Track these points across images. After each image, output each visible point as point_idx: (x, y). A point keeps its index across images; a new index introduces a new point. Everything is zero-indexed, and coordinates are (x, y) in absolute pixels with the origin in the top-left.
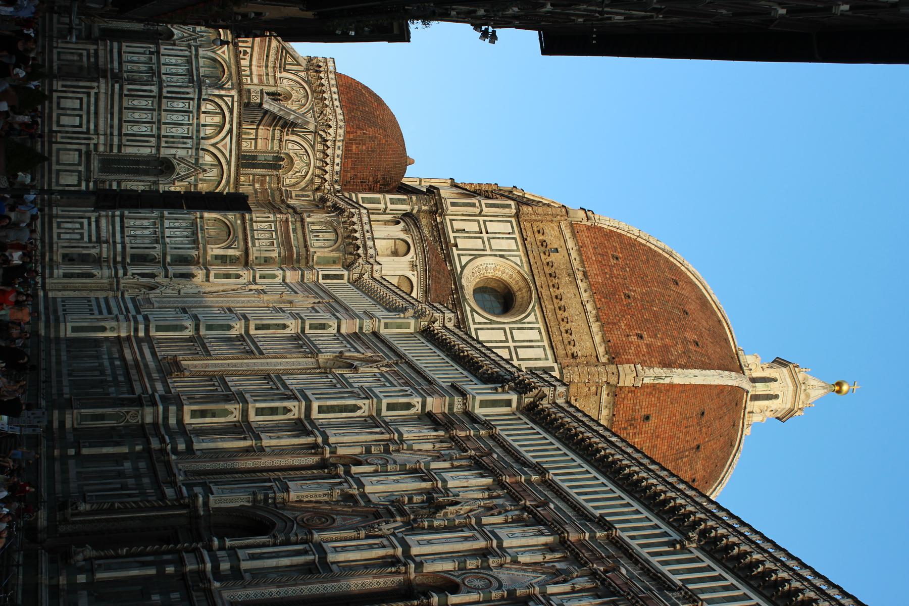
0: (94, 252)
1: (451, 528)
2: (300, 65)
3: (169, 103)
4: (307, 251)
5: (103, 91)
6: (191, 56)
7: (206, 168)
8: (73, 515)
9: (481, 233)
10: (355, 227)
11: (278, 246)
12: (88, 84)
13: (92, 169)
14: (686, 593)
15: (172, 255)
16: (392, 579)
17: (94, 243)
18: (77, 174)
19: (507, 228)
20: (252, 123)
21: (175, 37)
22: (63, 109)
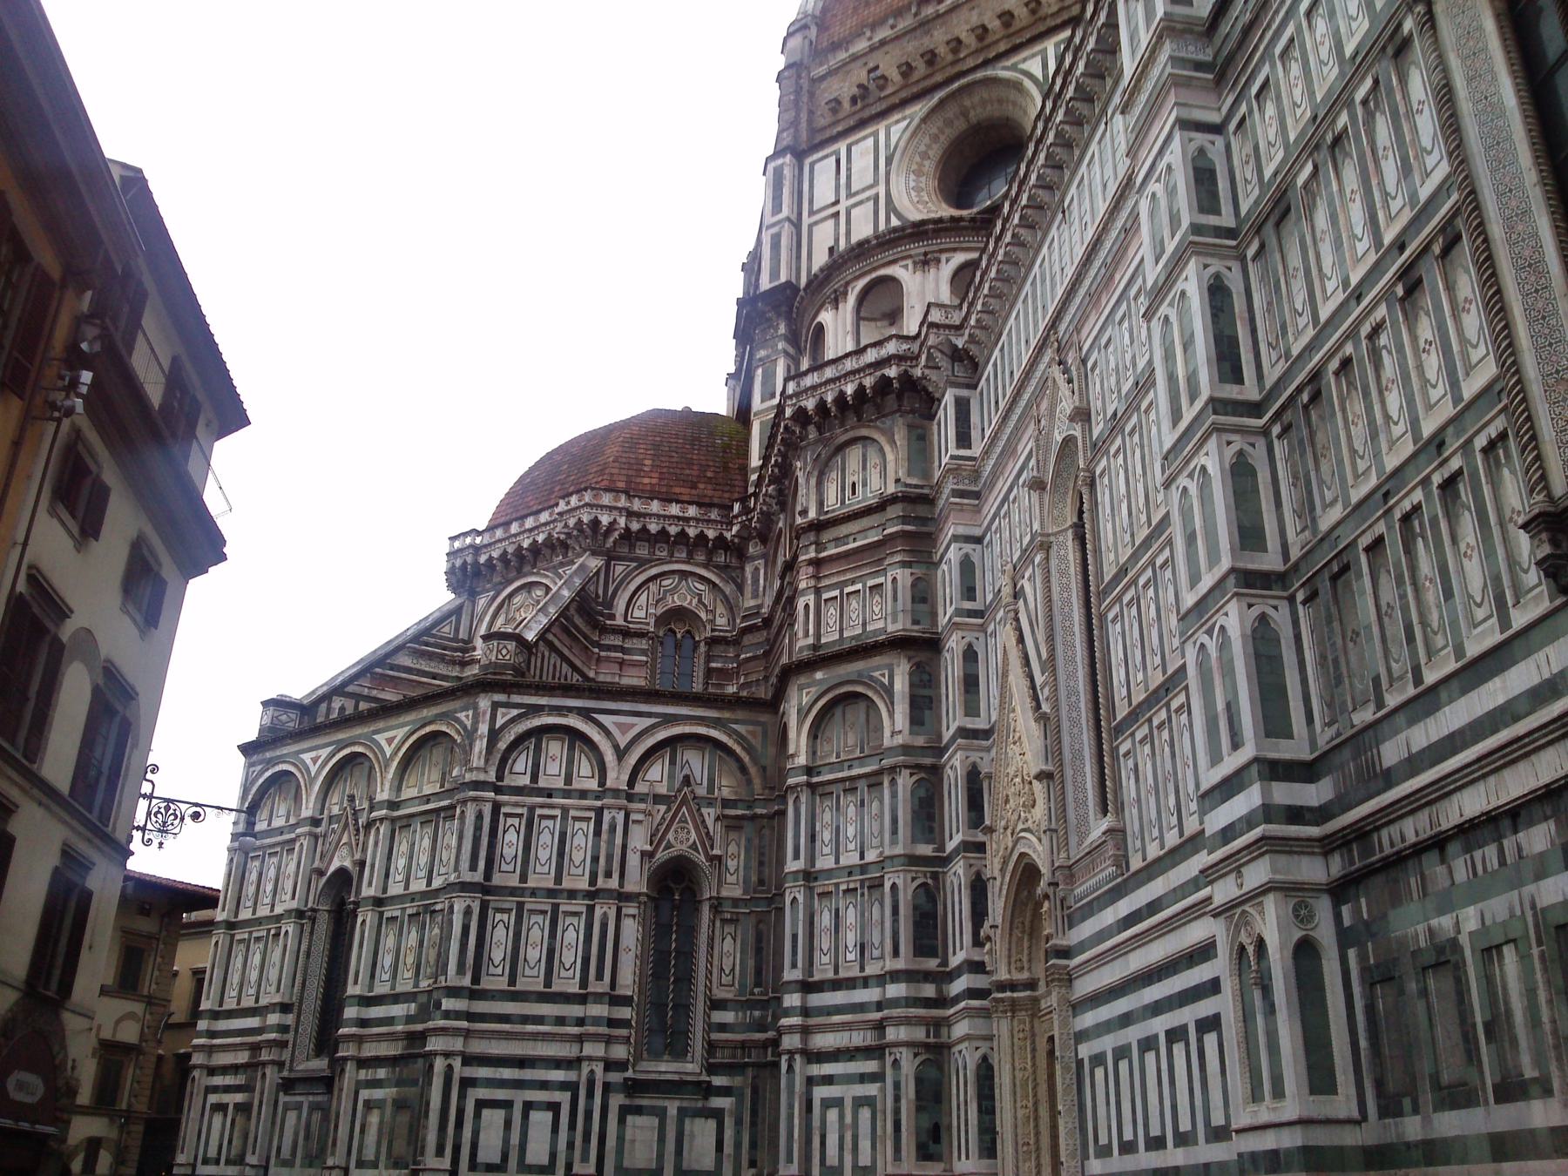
0: (908, 1064)
3: (504, 867)
4: (895, 499)
6: (393, 820)
7: (679, 778)
9: (838, 213)
10: (829, 398)
13: (676, 1077)
17: (883, 1067)
18: (687, 1121)
21: (347, 864)
22: (505, 1157)
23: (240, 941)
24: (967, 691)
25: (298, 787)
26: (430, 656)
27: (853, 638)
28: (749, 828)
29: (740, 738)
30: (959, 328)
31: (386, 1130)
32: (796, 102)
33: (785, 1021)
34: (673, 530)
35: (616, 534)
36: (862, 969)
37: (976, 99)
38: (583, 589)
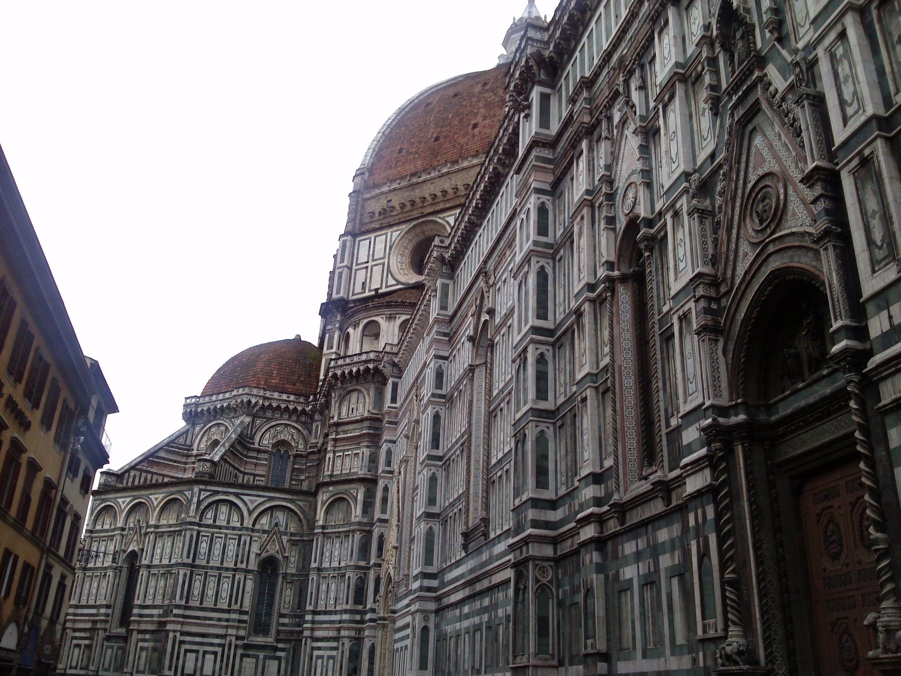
0: (347, 644)
2: (188, 430)
3: (200, 557)
4: (366, 419)
5: (179, 627)
6: (156, 533)
9: (367, 267)
13: (263, 644)
18: (267, 661)
20: (236, 476)
21: (136, 549)
23: (88, 576)
24: (383, 504)
26: (173, 453)
27: (346, 474)
28: (300, 545)
29: (300, 507)
30: (396, 354)
33: (305, 625)
34: (283, 406)
35: (258, 407)
36: (335, 608)
37: (428, 228)
38: (241, 433)
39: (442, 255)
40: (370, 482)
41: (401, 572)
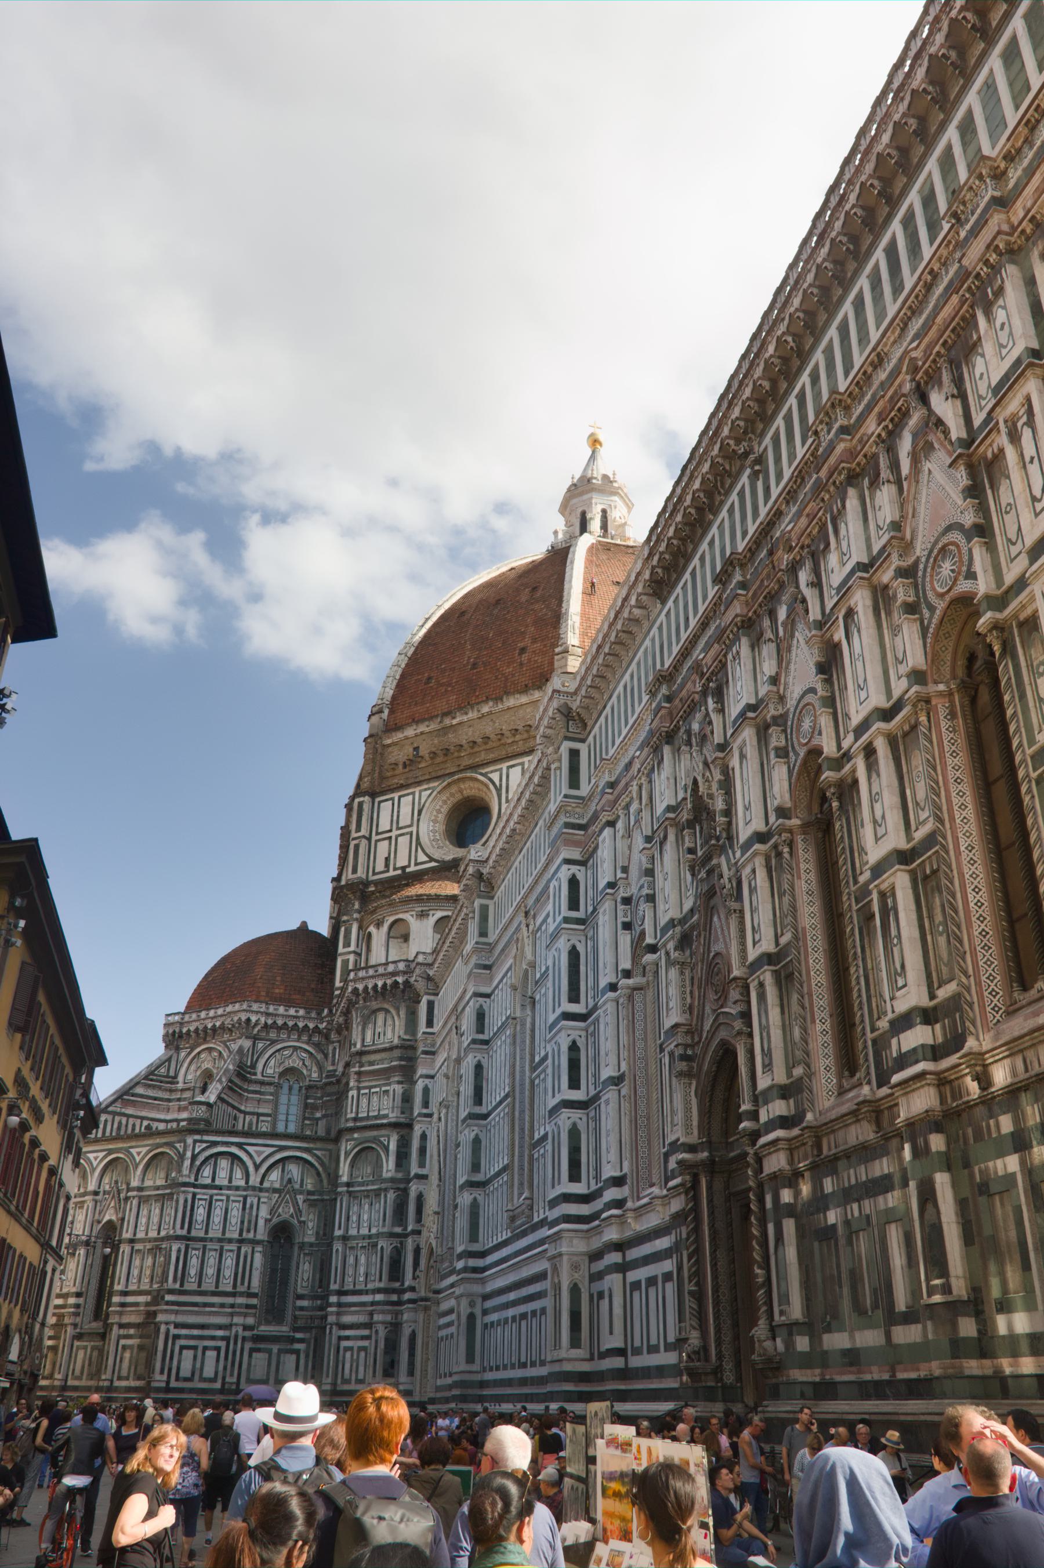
0: (382, 1333)
1: (727, 785)
3: (197, 1227)
4: (397, 1047)
5: (172, 1318)
6: (140, 1197)
8: (707, 1359)
9: (390, 838)
10: (370, 986)
11: (389, 1084)
12: (162, 1337)
14: (821, 422)
15: (393, 1225)
16: (800, 851)
19: (386, 808)
20: (235, 1118)
21: (114, 1218)
25: (85, 1171)
29: (318, 1157)
30: (430, 965)
31: (134, 1361)
32: (373, 761)
33: (330, 1309)
34: (290, 1024)
35: (259, 1027)
39: (478, 870)
40: (404, 1127)
41: (445, 1243)
